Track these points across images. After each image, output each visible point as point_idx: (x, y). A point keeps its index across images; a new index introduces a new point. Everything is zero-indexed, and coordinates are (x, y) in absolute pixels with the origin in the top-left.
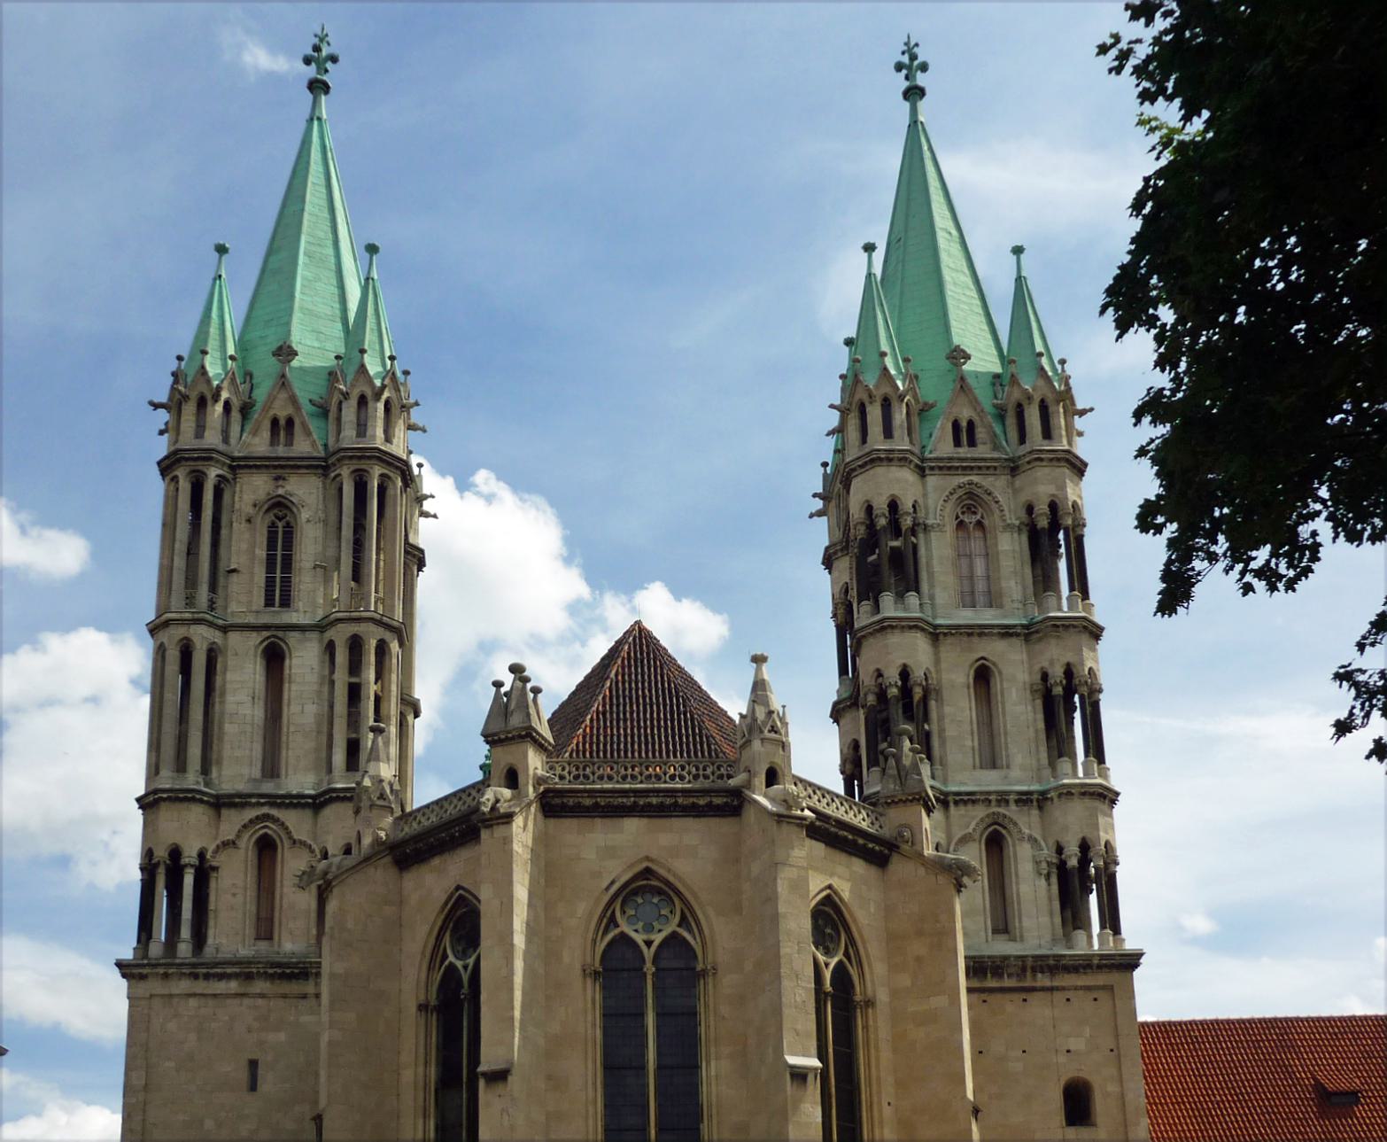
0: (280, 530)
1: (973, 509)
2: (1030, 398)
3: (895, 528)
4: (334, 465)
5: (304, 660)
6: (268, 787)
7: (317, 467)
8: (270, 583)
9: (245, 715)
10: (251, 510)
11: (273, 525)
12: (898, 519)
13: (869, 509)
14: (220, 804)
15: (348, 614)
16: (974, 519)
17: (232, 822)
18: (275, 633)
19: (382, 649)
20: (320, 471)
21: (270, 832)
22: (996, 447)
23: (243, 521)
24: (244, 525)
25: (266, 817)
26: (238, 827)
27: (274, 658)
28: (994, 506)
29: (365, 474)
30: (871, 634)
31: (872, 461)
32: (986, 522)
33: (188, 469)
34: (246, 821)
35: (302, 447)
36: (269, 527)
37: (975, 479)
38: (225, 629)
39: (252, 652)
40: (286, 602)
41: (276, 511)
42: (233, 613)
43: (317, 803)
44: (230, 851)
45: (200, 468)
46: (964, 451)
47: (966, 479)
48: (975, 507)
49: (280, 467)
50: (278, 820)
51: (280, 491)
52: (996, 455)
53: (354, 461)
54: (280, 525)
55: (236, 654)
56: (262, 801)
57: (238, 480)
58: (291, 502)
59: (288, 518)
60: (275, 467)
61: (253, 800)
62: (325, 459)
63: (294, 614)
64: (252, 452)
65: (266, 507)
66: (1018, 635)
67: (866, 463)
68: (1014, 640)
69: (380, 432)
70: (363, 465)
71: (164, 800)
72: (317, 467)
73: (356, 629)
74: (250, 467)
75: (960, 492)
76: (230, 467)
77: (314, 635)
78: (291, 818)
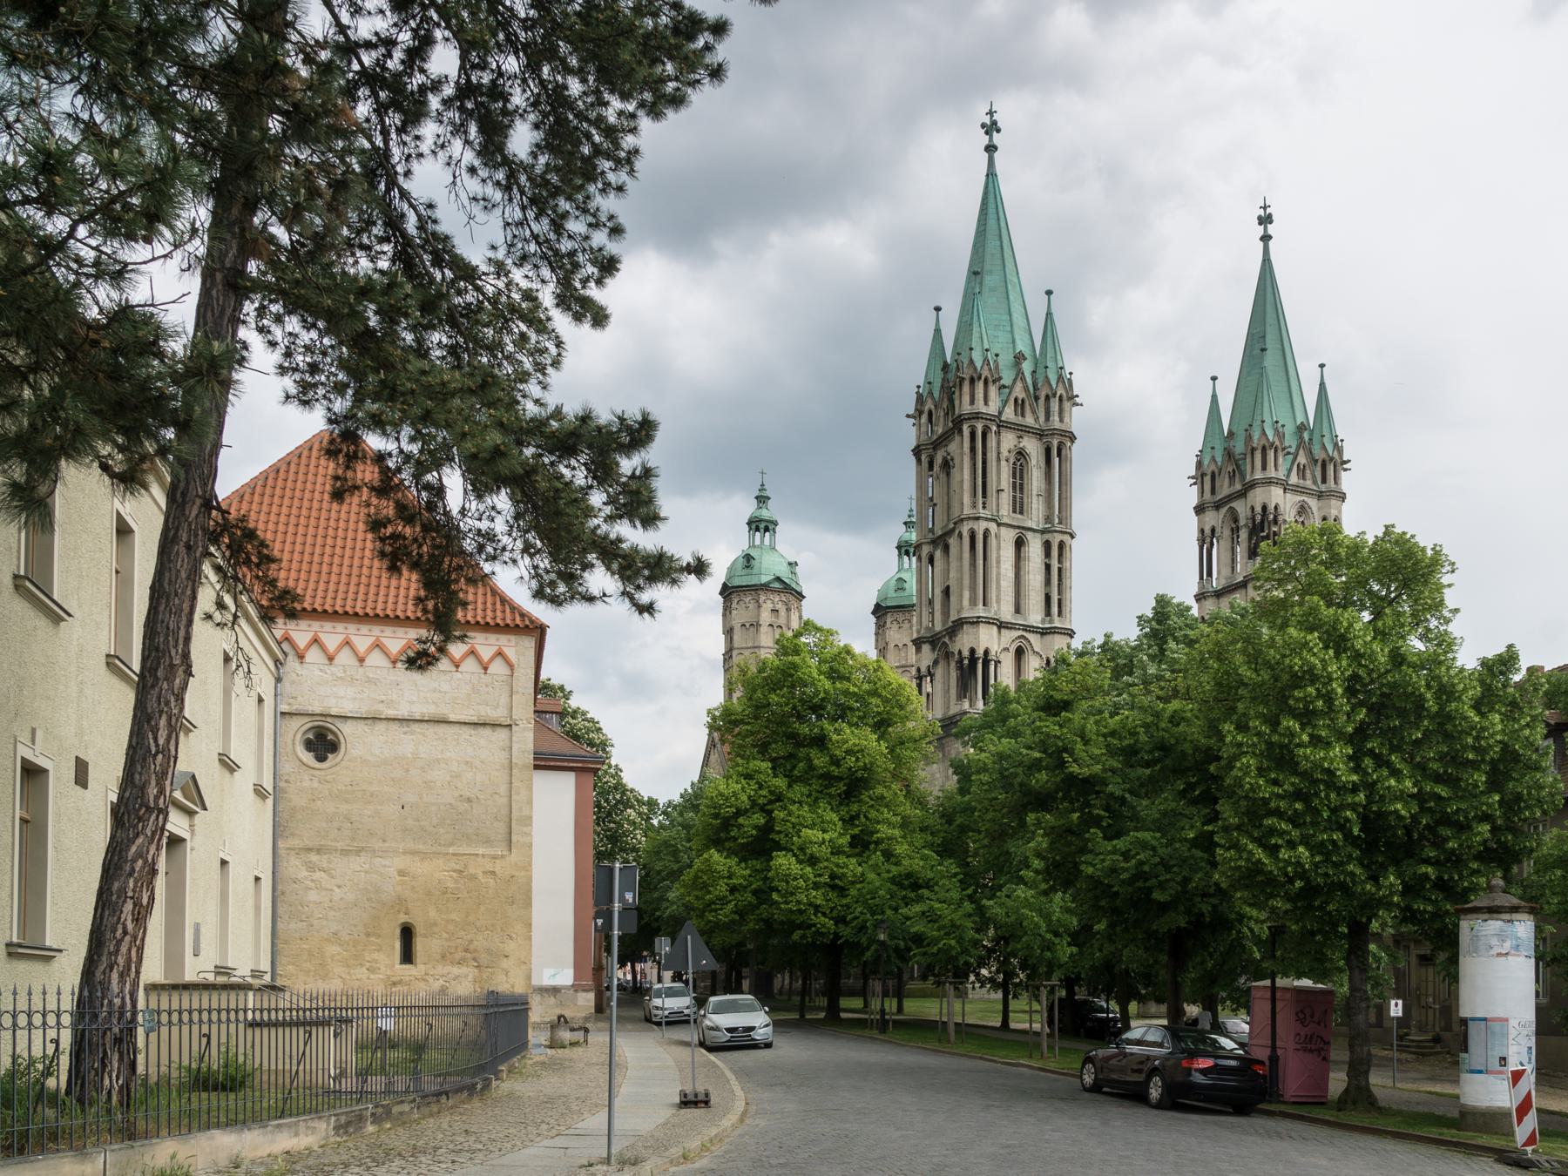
3: (1275, 522)
5: (1034, 548)
8: (1014, 497)
13: (1264, 508)
14: (1002, 626)
19: (1061, 545)
22: (1315, 482)
25: (1022, 637)
27: (1020, 543)
35: (1029, 420)
38: (999, 525)
49: (1021, 430)
69: (1057, 418)
76: (998, 426)
77: (1038, 535)
78: (1032, 637)
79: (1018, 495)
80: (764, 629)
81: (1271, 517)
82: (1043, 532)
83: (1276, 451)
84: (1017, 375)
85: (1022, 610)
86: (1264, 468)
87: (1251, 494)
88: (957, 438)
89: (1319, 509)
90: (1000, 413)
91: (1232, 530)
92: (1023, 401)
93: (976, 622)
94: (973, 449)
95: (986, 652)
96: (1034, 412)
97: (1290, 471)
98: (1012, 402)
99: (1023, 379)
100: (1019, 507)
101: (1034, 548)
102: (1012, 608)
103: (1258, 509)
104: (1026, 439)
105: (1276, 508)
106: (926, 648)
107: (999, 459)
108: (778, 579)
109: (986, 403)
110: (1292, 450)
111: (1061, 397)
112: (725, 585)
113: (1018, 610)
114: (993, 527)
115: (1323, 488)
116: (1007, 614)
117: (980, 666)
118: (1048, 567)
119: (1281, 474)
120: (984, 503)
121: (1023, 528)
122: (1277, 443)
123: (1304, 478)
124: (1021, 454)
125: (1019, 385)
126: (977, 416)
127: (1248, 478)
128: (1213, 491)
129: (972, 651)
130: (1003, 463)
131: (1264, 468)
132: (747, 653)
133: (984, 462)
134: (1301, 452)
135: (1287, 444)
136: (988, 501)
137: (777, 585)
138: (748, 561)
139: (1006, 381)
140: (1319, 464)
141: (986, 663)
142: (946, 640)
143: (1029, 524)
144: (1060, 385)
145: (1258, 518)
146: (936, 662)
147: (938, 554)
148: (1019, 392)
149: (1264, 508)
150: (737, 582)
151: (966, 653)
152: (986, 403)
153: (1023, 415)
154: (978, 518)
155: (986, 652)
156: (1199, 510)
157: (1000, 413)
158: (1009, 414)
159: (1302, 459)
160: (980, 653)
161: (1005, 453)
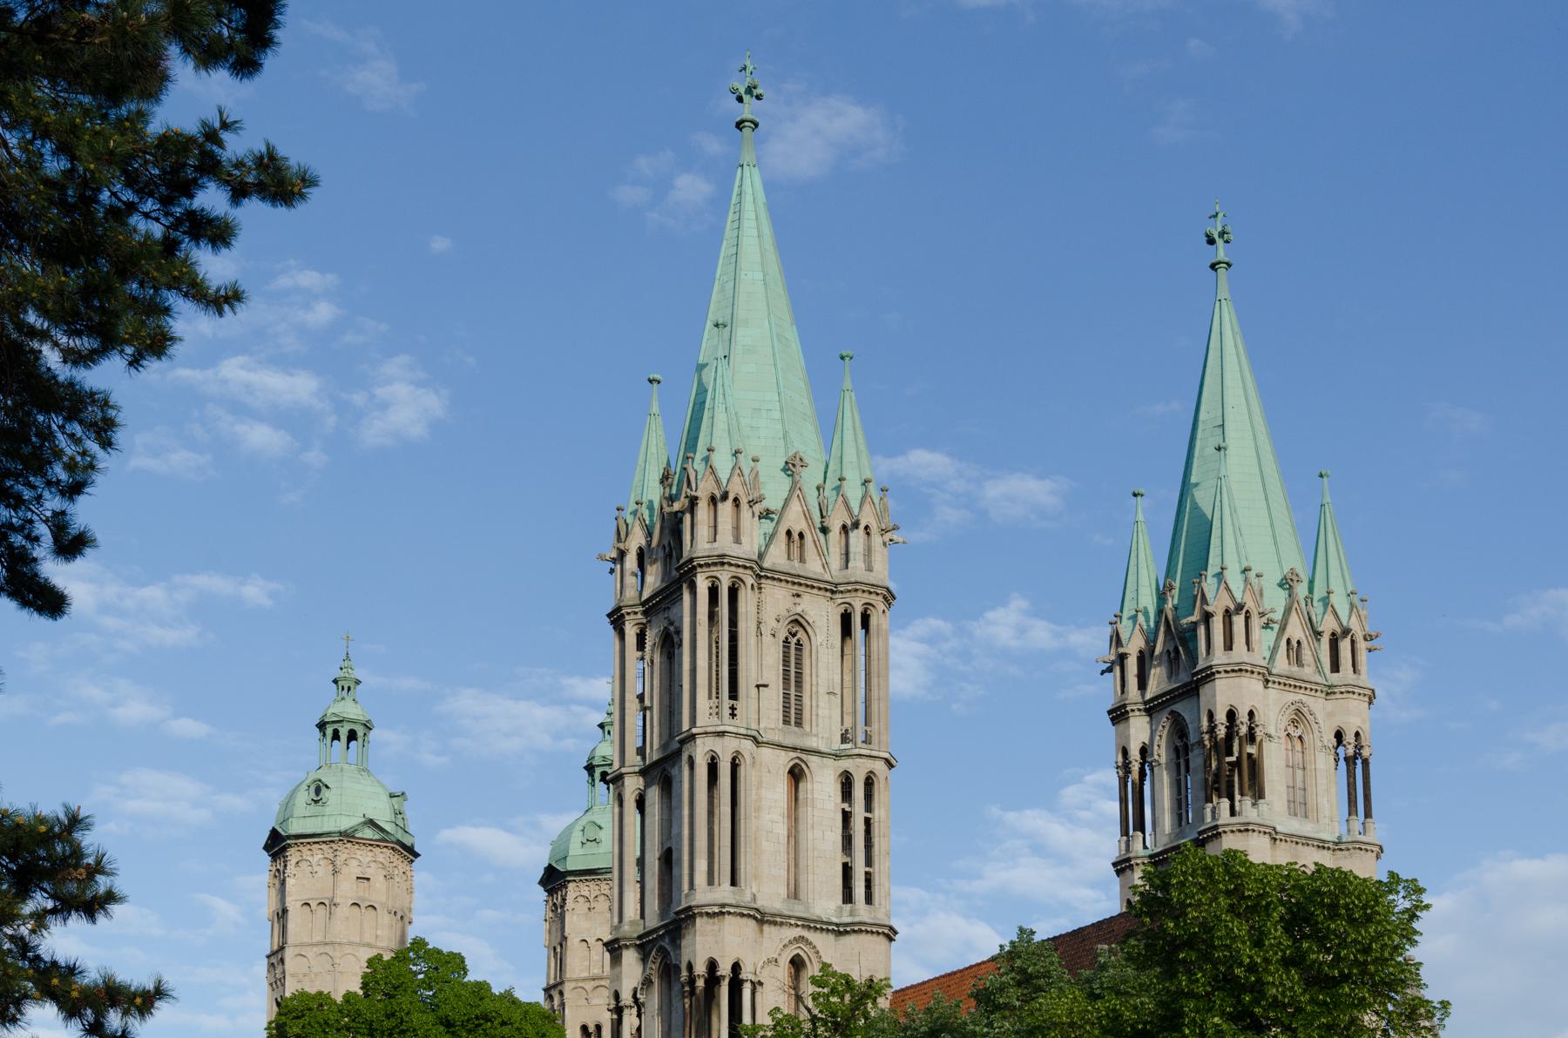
0: (793, 646)
1: (1296, 724)
2: (1346, 632)
3: (1251, 737)
4: (842, 592)
5: (823, 785)
6: (799, 911)
7: (826, 590)
8: (786, 696)
9: (779, 834)
10: (774, 623)
11: (786, 641)
12: (1253, 729)
13: (1231, 715)
14: (763, 919)
15: (868, 751)
16: (1298, 732)
17: (776, 942)
18: (799, 755)
20: (828, 594)
21: (802, 953)
22: (1319, 671)
23: (769, 635)
24: (771, 638)
26: (781, 946)
28: (1313, 724)
29: (871, 607)
30: (1232, 831)
31: (1241, 670)
32: (1305, 738)
33: (731, 574)
34: (786, 942)
35: (813, 567)
36: (784, 642)
37: (1304, 698)
38: (757, 742)
39: (781, 772)
40: (799, 723)
41: (790, 627)
42: (766, 729)
43: (841, 931)
44: (772, 967)
45: (740, 575)
46: (1295, 668)
47: (1293, 697)
48: (1298, 722)
49: (799, 583)
50: (811, 944)
51: (799, 609)
52: (1319, 679)
53: (866, 595)
54: (794, 641)
55: (769, 771)
56: (799, 923)
57: (763, 590)
58: (807, 621)
59: (798, 636)
60: (794, 583)
61: (793, 922)
62: (836, 585)
63: (814, 739)
64: (774, 564)
65: (787, 622)
66: (1329, 848)
67: (1233, 671)
68: (1325, 852)
70: (873, 599)
71: (729, 913)
72: (826, 590)
73: (872, 766)
74: (773, 579)
75: (1293, 707)
76: (759, 577)
77: (829, 762)
79: (793, 692)
80: (343, 911)
81: (1244, 730)
82: (837, 756)
83: (1247, 618)
84: (792, 491)
85: (802, 895)
86: (1229, 646)
87: (1205, 691)
88: (686, 597)
89: (1330, 715)
90: (761, 556)
91: (1176, 750)
92: (801, 535)
93: (720, 912)
94: (713, 617)
95: (736, 967)
96: (821, 554)
97: (1274, 650)
98: (782, 536)
99: (803, 499)
100: (793, 714)
101: (823, 785)
102: (783, 891)
103: (1221, 717)
104: (806, 597)
105: (1251, 714)
106: (630, 957)
107: (760, 633)
108: (371, 823)
109: (737, 540)
110: (1278, 616)
111: (867, 527)
112: (274, 832)
113: (794, 894)
114: (747, 746)
115: (1334, 678)
116: (771, 896)
117: (724, 991)
118: (846, 817)
119: (1259, 656)
120: (733, 708)
121: (802, 750)
122: (1250, 605)
123: (1299, 662)
124: (798, 622)
125: (795, 507)
126: (721, 561)
127: (1201, 665)
128: (1142, 685)
129: (712, 965)
130: (767, 638)
131: (1229, 646)
132: (310, 953)
133: (733, 638)
134: (1294, 618)
135: (1267, 605)
136: (739, 705)
137: (369, 833)
138: (318, 791)
139: (772, 502)
140: (1325, 640)
141: (736, 985)
142: (666, 943)
143: (812, 743)
144: (867, 507)
145: (1221, 732)
146: (647, 982)
147: (654, 795)
148: (795, 519)
149: (1231, 715)
150: (295, 827)
151: (700, 969)
152: (737, 540)
153: (802, 560)
154: (721, 734)
155: (736, 967)
156: (1119, 715)
157: (761, 556)
158: (777, 557)
159: (1296, 630)
160: (725, 969)
161: (770, 624)
